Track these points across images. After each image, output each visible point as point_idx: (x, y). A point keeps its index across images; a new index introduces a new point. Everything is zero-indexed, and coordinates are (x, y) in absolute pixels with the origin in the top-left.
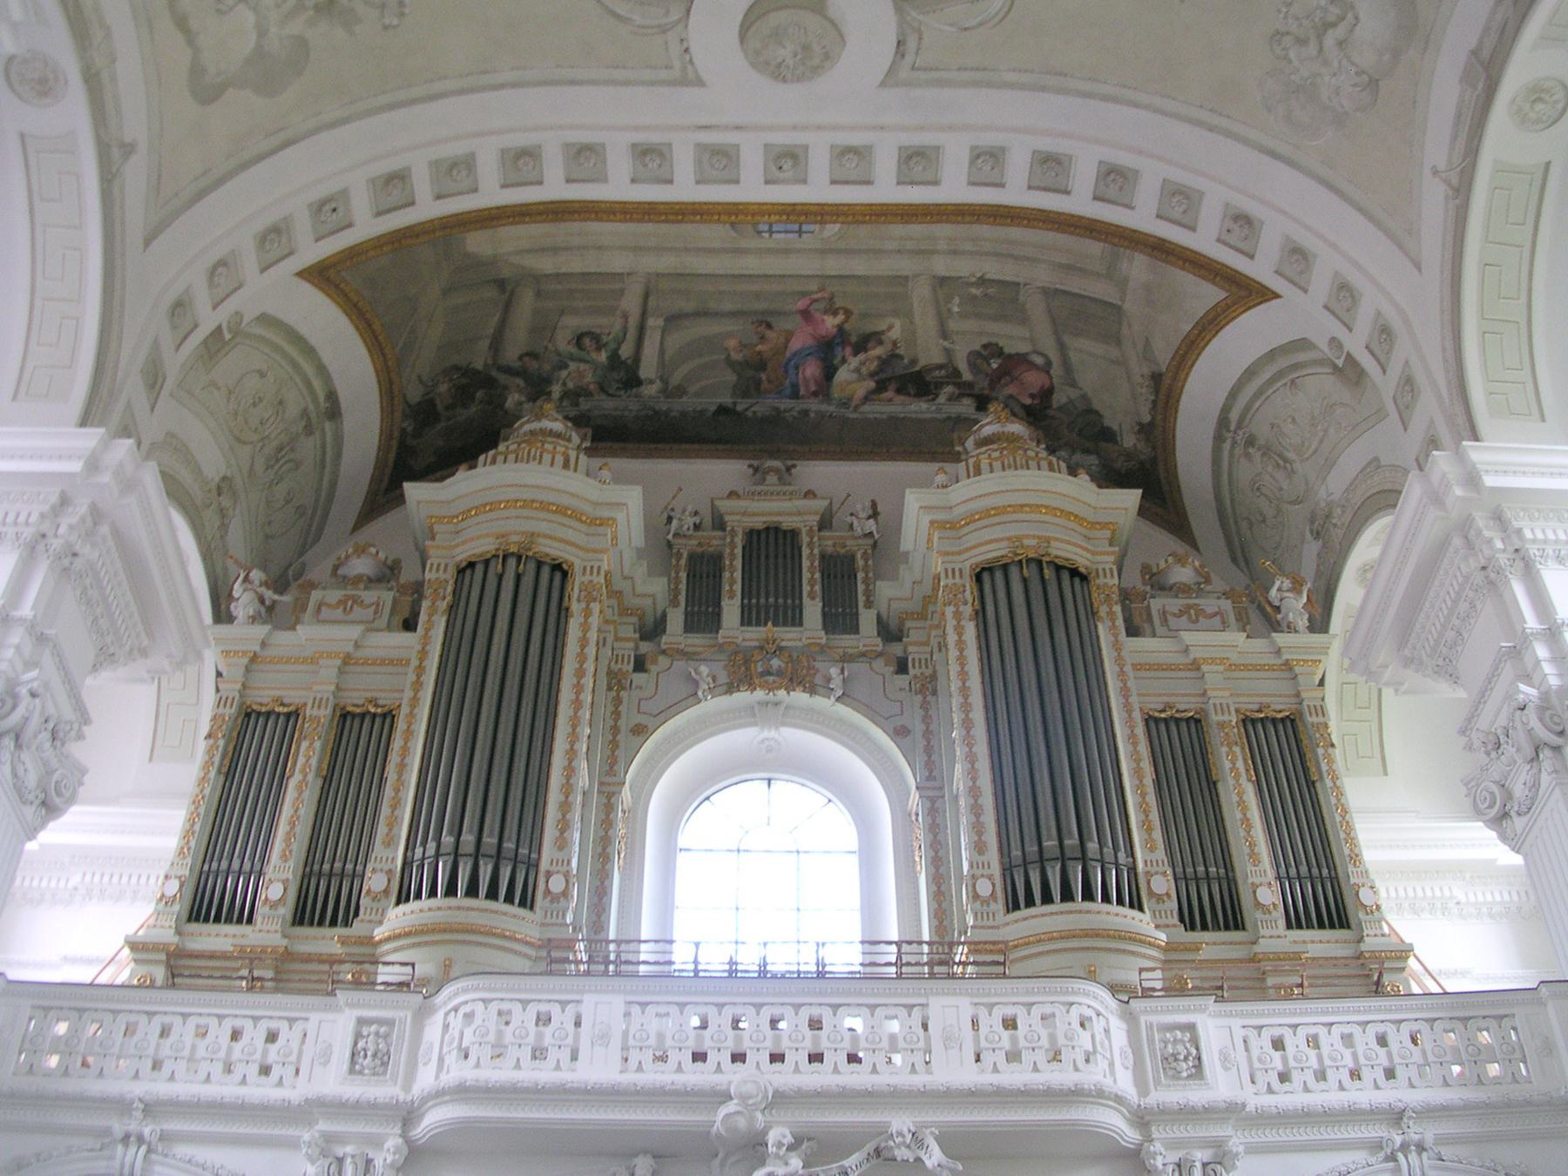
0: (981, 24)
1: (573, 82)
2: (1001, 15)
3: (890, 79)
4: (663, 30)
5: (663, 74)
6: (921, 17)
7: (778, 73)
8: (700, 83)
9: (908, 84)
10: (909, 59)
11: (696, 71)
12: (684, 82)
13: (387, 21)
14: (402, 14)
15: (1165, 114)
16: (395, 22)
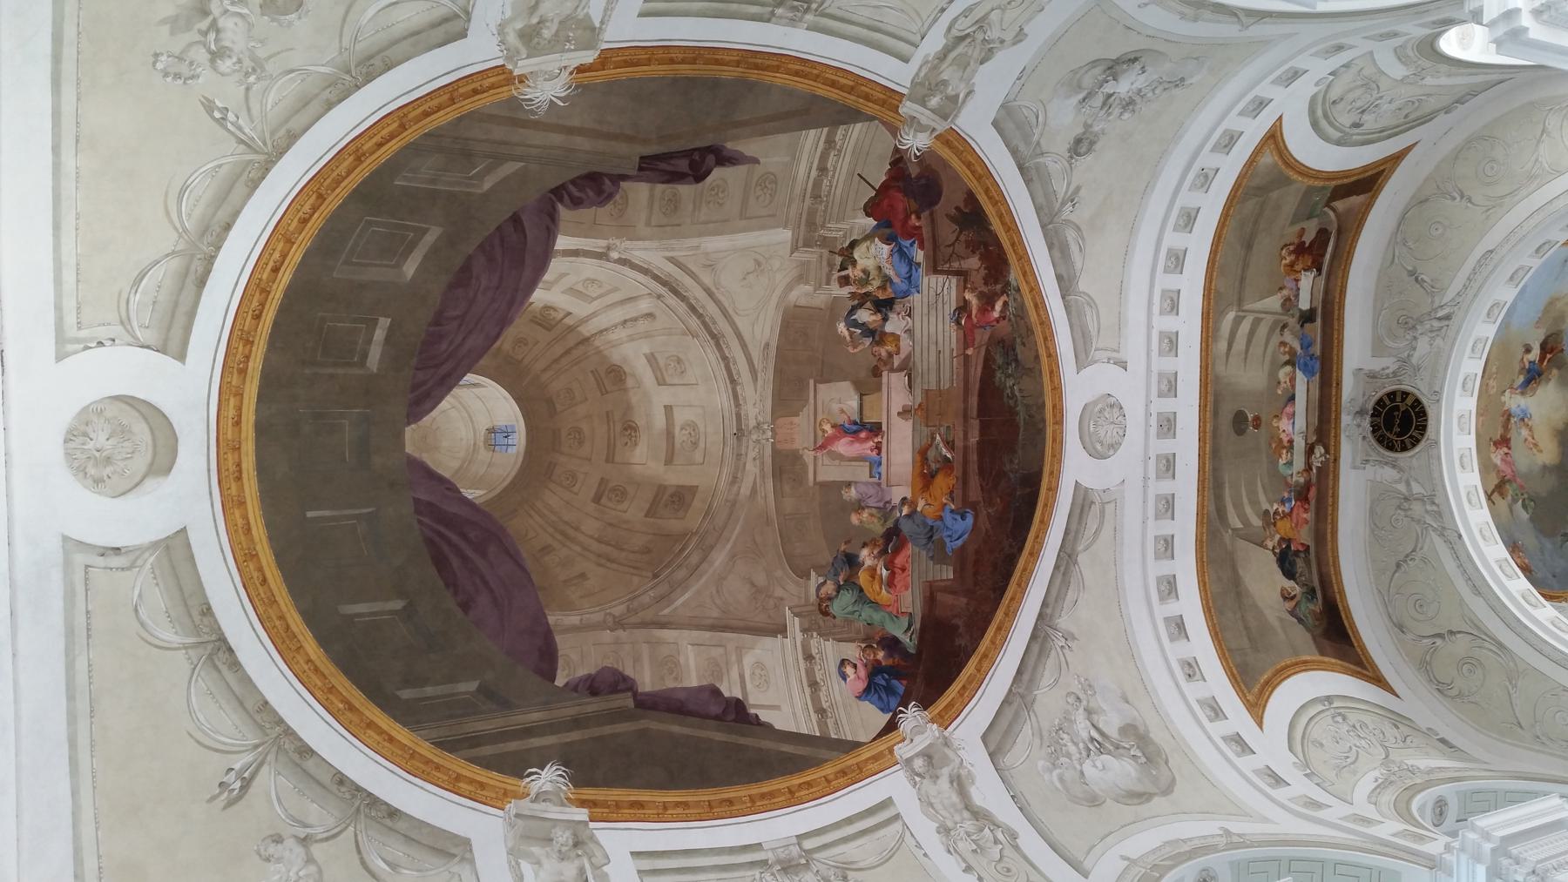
0: (142, 624)
1: (57, 227)
2: (150, 639)
3: (71, 545)
4: (125, 322)
5: (70, 319)
6: (148, 566)
7: (76, 434)
8: (60, 357)
9: (67, 564)
10: (100, 561)
11: (76, 352)
12: (61, 338)
13: (163, 58)
14: (166, 75)
15: (75, 825)
16: (159, 66)
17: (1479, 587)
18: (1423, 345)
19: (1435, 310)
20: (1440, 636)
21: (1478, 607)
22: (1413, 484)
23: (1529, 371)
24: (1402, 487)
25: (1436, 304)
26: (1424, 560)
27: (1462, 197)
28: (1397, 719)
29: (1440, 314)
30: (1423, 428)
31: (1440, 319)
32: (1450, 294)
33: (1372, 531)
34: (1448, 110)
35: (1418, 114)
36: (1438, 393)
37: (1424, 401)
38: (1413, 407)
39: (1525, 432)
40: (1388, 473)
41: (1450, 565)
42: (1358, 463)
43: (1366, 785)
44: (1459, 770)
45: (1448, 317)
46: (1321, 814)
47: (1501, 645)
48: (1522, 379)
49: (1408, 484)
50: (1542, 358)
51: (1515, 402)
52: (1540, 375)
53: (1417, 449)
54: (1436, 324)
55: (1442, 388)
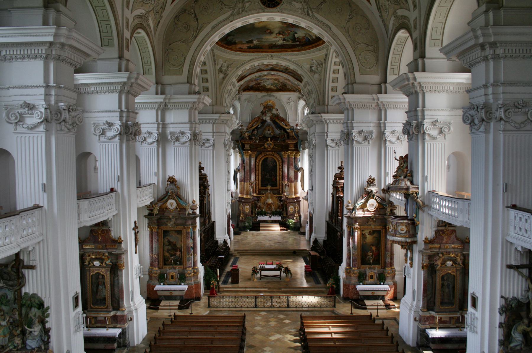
17: (215, 29)
18: (298, 5)
19: (311, 10)
20: (195, 16)
21: (208, 29)
22: (249, 3)
25: (313, 10)
26: (222, 9)
27: (350, 19)
28: (163, 8)
29: (310, 12)
30: (269, 7)
31: (308, 11)
32: (316, 15)
34: (381, 16)
35: (382, 9)
36: (281, 11)
37: (279, 7)
38: (276, 2)
43: (138, 12)
44: (151, 32)
45: (308, 14)
46: (125, 8)
47: (196, 37)
53: (261, 4)
54: (306, 10)
55: (283, 13)
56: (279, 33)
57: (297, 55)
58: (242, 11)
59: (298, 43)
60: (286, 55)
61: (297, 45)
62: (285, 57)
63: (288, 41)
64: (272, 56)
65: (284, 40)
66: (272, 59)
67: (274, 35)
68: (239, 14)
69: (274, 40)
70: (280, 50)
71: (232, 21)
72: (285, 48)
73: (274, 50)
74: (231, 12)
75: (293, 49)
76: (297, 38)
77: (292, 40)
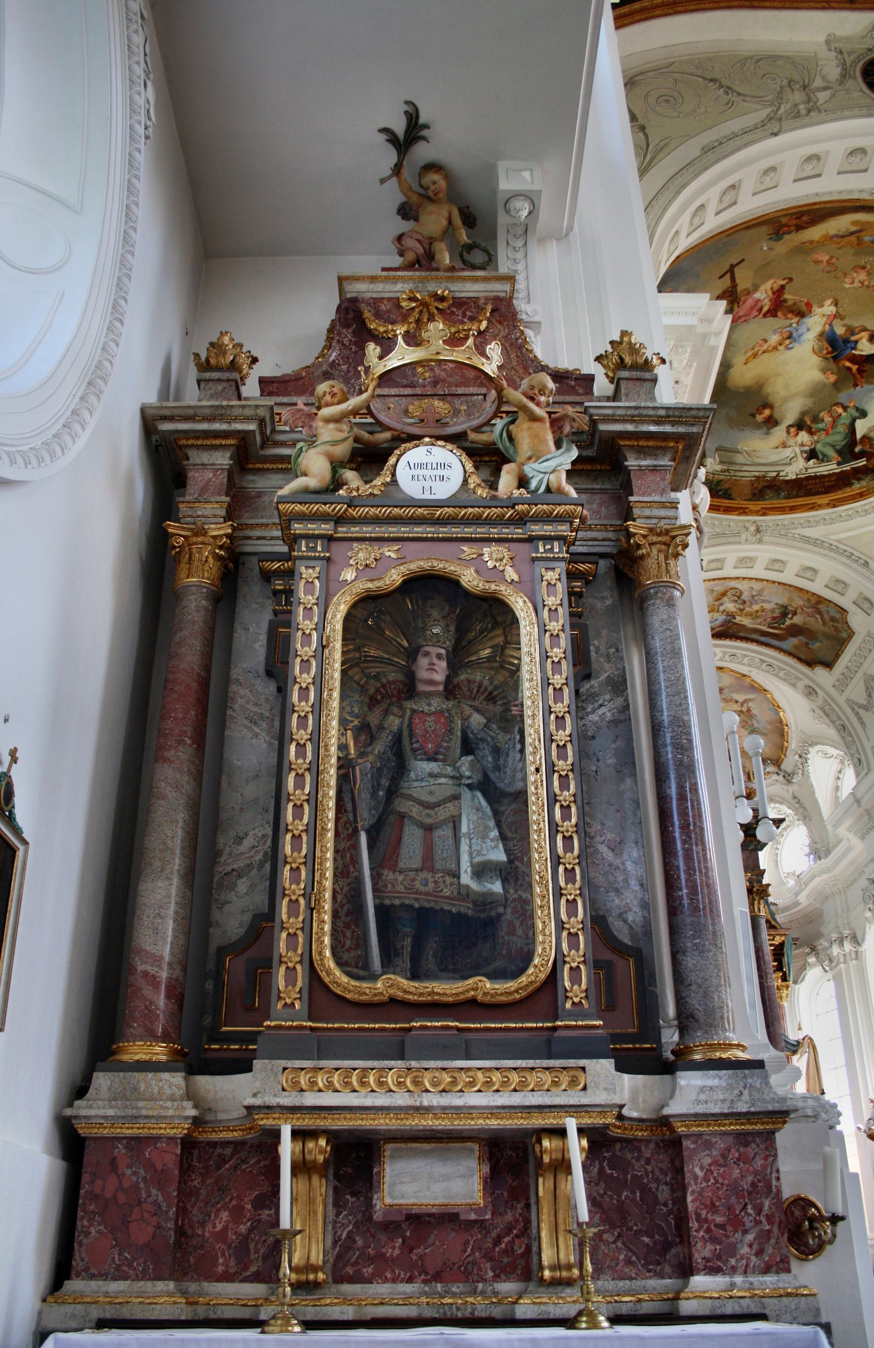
21: (690, 150)
22: (828, 93)
23: (846, 341)
24: (818, 83)
26: (730, 104)
33: (751, 58)
39: (774, 339)
40: (834, 72)
41: (735, 125)
42: (840, 45)
48: (840, 331)
49: (826, 88)
50: (854, 359)
51: (814, 325)
52: (835, 359)
56: (800, 425)
57: (850, 517)
58: (809, 111)
59: (862, 462)
60: (809, 524)
61: (857, 474)
62: (806, 532)
63: (823, 459)
64: (758, 531)
65: (812, 454)
66: (760, 541)
67: (779, 433)
68: (798, 116)
69: (773, 458)
70: (792, 502)
71: (776, 134)
72: (809, 493)
73: (767, 504)
74: (769, 110)
75: (839, 495)
76: (864, 437)
77: (839, 452)
